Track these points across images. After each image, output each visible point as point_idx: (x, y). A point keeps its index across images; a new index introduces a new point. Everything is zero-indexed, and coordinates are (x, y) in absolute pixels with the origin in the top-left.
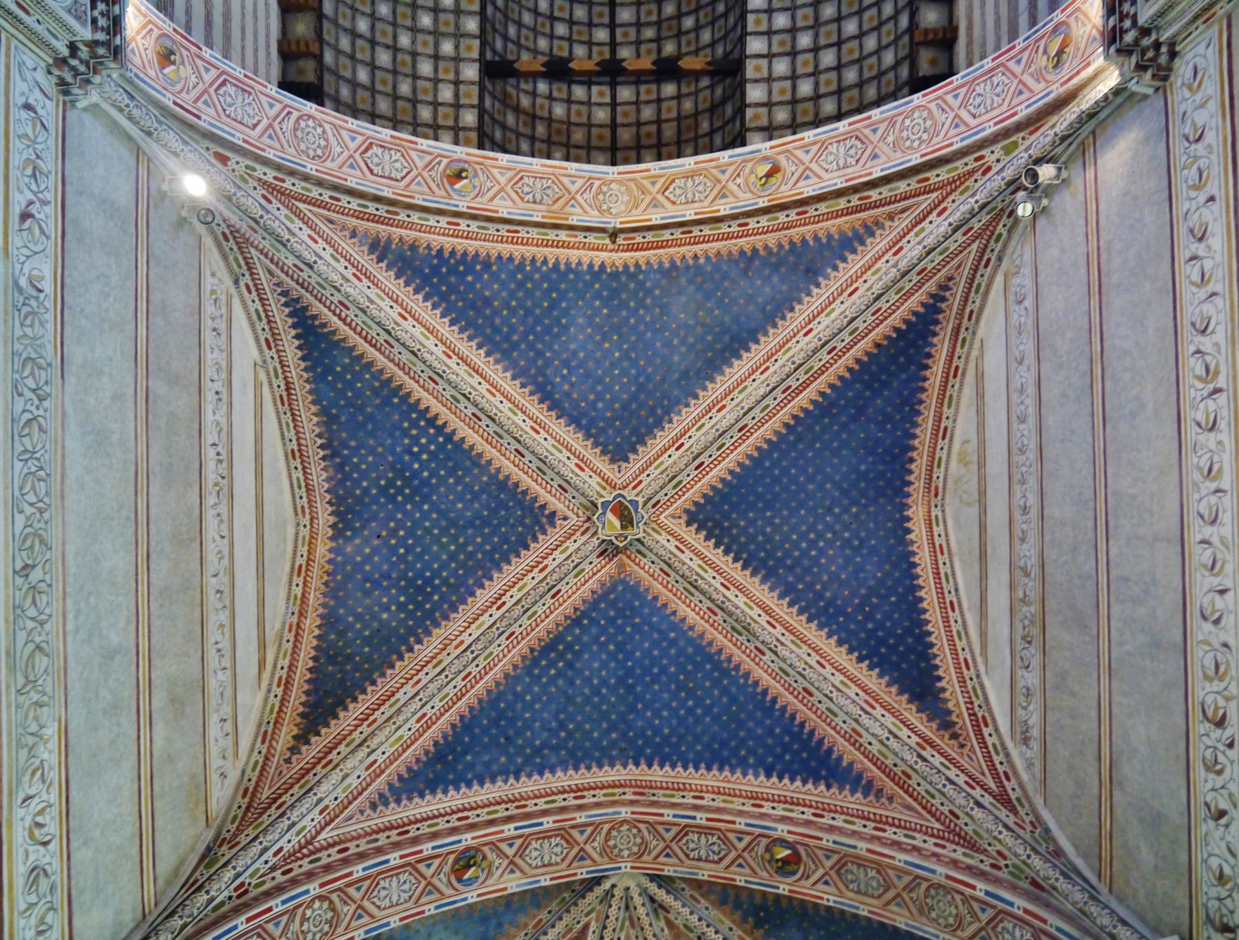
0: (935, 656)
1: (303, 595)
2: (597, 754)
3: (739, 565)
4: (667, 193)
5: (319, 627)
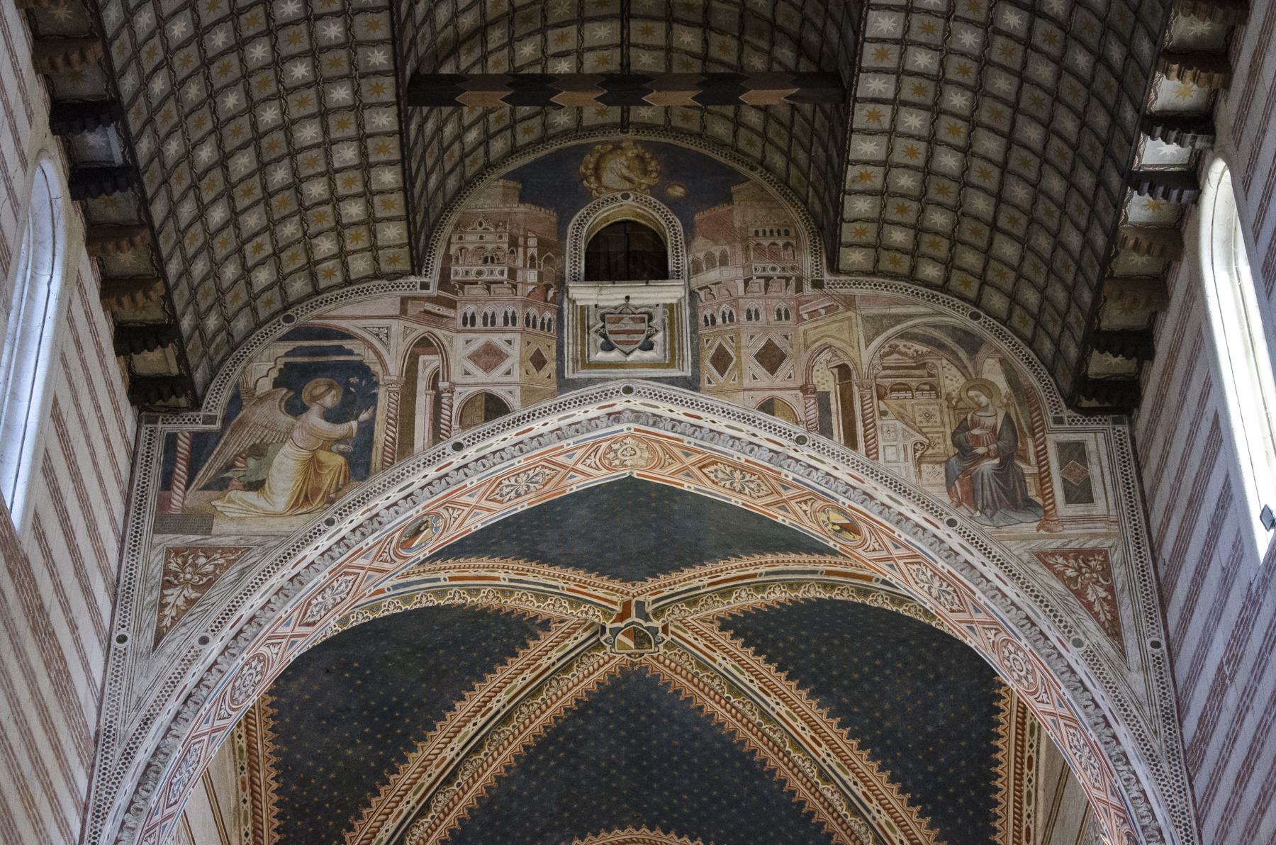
0: (997, 817)
1: (249, 746)
2: (605, 823)
3: (783, 675)
4: (705, 470)
5: (276, 779)
